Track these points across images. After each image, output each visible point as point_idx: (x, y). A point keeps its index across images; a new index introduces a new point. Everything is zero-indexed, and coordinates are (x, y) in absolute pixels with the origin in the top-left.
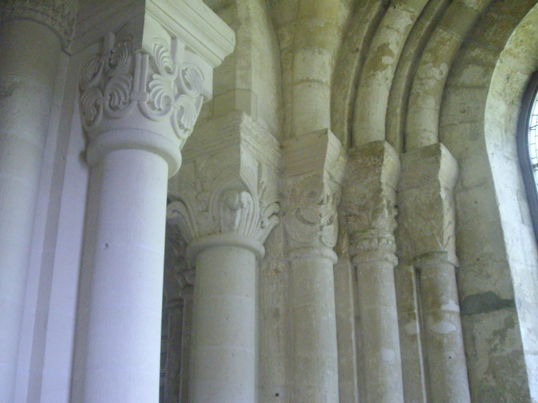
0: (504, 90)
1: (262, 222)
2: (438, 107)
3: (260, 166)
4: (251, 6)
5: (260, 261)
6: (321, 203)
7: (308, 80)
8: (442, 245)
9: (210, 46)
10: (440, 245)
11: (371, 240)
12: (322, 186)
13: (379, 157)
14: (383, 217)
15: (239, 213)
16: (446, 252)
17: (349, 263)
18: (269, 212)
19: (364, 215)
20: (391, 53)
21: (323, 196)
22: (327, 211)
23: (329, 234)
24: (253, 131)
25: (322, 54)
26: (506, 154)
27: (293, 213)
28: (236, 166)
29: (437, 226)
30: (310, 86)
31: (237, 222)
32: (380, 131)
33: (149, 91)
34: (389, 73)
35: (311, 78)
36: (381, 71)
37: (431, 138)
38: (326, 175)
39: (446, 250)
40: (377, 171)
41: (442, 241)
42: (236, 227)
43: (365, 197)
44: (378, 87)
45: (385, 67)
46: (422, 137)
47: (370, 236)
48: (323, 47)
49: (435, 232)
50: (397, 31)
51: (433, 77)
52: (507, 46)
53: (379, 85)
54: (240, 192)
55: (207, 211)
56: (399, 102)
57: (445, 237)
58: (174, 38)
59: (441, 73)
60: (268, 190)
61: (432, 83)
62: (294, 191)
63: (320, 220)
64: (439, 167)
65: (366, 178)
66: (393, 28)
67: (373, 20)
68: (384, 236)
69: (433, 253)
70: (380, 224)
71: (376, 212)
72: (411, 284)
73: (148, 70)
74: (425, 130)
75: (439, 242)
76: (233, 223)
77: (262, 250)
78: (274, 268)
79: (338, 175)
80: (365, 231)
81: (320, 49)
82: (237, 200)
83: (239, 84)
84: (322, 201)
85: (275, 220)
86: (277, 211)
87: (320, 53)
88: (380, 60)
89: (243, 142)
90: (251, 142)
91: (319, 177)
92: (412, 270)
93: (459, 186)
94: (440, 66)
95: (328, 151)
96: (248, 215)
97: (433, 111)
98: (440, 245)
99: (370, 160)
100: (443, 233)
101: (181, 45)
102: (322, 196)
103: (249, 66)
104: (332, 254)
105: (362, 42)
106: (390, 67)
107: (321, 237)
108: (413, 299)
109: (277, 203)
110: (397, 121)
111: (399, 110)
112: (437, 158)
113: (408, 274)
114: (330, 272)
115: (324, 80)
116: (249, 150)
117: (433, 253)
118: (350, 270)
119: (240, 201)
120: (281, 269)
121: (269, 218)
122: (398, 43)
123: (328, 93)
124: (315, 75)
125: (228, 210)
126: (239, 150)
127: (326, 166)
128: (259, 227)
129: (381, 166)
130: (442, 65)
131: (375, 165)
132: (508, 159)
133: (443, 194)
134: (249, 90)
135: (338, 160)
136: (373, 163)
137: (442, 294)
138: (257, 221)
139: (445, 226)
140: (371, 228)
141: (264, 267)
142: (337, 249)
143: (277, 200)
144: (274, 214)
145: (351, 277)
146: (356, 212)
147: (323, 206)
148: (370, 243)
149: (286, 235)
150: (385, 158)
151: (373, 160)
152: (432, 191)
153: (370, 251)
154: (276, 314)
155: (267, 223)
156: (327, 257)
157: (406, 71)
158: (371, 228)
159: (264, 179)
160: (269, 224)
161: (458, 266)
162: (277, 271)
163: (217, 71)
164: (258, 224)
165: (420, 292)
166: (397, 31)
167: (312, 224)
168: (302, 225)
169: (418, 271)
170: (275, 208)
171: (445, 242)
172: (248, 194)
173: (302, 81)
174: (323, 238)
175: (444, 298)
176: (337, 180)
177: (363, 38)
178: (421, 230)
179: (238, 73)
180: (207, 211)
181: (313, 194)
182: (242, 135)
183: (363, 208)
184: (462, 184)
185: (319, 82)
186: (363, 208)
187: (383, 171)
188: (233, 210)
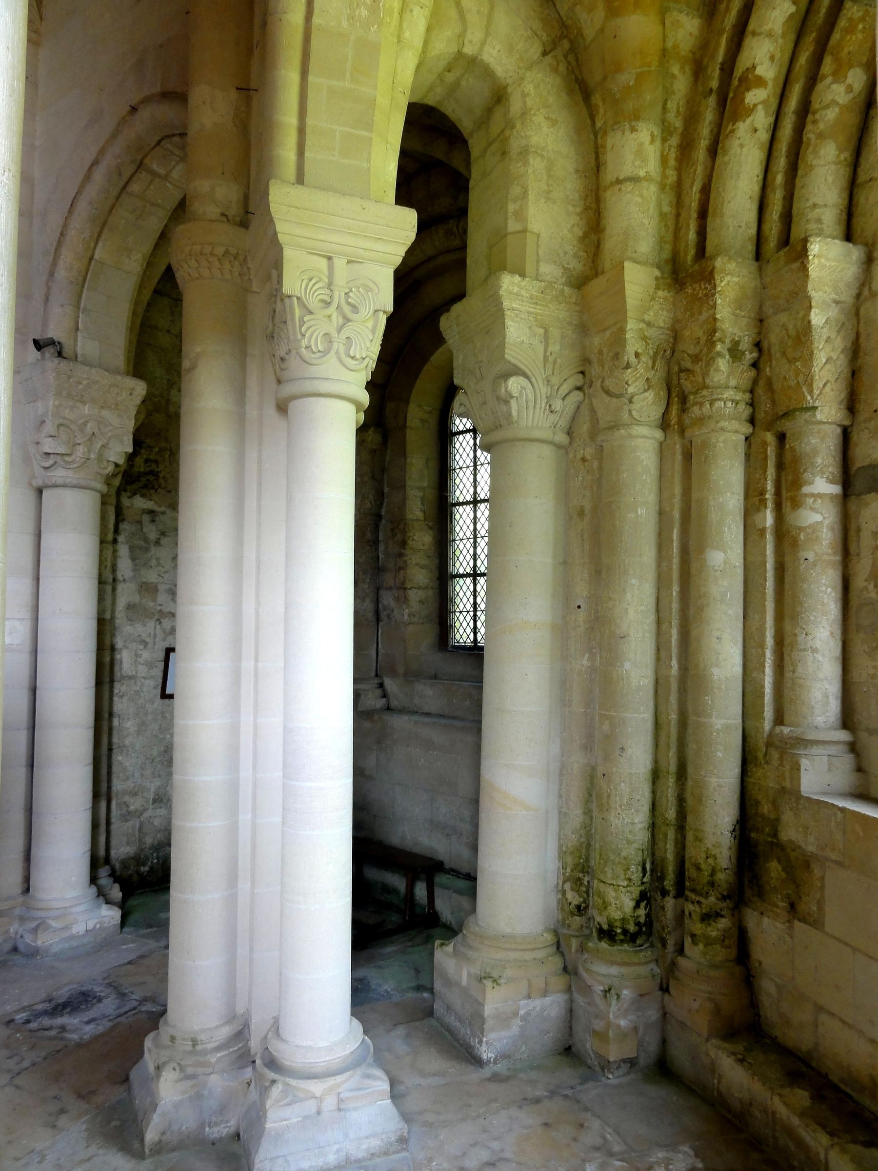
1: (550, 406)
2: (846, 155)
6: (628, 366)
7: (619, 182)
8: (812, 397)
9: (379, 247)
10: (809, 398)
11: (701, 404)
13: (709, 281)
14: (717, 370)
15: (513, 404)
16: (815, 408)
17: (677, 438)
19: (697, 368)
20: (760, 82)
24: (523, 292)
25: (637, 131)
27: (599, 384)
29: (804, 370)
30: (620, 189)
31: (514, 413)
32: (740, 227)
33: (303, 335)
34: (761, 119)
35: (621, 178)
36: (744, 121)
37: (823, 217)
38: (632, 325)
39: (817, 404)
40: (711, 303)
41: (811, 392)
42: (515, 419)
43: (699, 342)
44: (739, 150)
45: (750, 111)
46: (807, 220)
47: (700, 400)
48: (637, 118)
49: (801, 379)
50: (770, 35)
51: (834, 102)
53: (741, 146)
55: (485, 403)
56: (781, 162)
57: (818, 384)
58: (330, 258)
59: (849, 89)
60: (559, 361)
61: (831, 114)
62: (601, 352)
63: (626, 390)
64: (807, 276)
65: (700, 313)
66: (759, 34)
67: (734, 26)
68: (720, 396)
69: (795, 410)
70: (716, 379)
71: (710, 361)
72: (765, 459)
73: (297, 312)
74: (815, 206)
75: (806, 393)
76: (510, 414)
78: (581, 456)
79: (661, 315)
80: (696, 393)
81: (633, 123)
82: (503, 390)
83: (513, 226)
84: (628, 363)
85: (577, 396)
86: (579, 384)
87: (633, 130)
88: (743, 100)
89: (507, 313)
90: (522, 309)
91: (622, 330)
92: (770, 437)
93: (866, 292)
94: (846, 77)
95: (628, 292)
96: (527, 402)
97: (833, 167)
98: (809, 398)
99: (700, 287)
100: (812, 380)
101: (340, 263)
102: (626, 358)
103: (525, 195)
105: (718, 72)
106: (760, 107)
107: (630, 411)
108: (766, 479)
109: (582, 373)
110: (777, 198)
111: (779, 179)
112: (803, 262)
113: (765, 444)
115: (642, 174)
116: (521, 318)
117: (795, 410)
118: (678, 447)
119: (506, 391)
120: (588, 457)
122: (772, 58)
125: (502, 402)
128: (547, 412)
129: (714, 295)
130: (851, 73)
131: (706, 295)
133: (817, 318)
134: (524, 231)
135: (653, 299)
136: (705, 292)
137: (804, 471)
138: (543, 405)
139: (816, 369)
140: (705, 387)
141: (571, 456)
143: (581, 369)
145: (679, 457)
146: (688, 364)
147: (629, 370)
148: (700, 409)
149: (593, 411)
150: (718, 282)
151: (703, 287)
152: (802, 313)
153: (701, 420)
155: (558, 405)
156: (637, 437)
157: (793, 103)
158: (705, 387)
159: (555, 348)
161: (847, 423)
162: (584, 460)
164: (545, 409)
165: (780, 466)
166: (770, 35)
167: (619, 396)
168: (607, 399)
169: (782, 438)
170: (578, 380)
171: (816, 392)
172: (521, 380)
173: (612, 184)
174: (634, 413)
175: (807, 476)
176: (662, 325)
177: (718, 66)
178: (785, 378)
179: (511, 207)
180: (485, 403)
181: (617, 356)
182: (506, 304)
183: (696, 359)
184: (870, 288)
185: (635, 179)
186: (696, 359)
187: (719, 301)
188: (507, 402)
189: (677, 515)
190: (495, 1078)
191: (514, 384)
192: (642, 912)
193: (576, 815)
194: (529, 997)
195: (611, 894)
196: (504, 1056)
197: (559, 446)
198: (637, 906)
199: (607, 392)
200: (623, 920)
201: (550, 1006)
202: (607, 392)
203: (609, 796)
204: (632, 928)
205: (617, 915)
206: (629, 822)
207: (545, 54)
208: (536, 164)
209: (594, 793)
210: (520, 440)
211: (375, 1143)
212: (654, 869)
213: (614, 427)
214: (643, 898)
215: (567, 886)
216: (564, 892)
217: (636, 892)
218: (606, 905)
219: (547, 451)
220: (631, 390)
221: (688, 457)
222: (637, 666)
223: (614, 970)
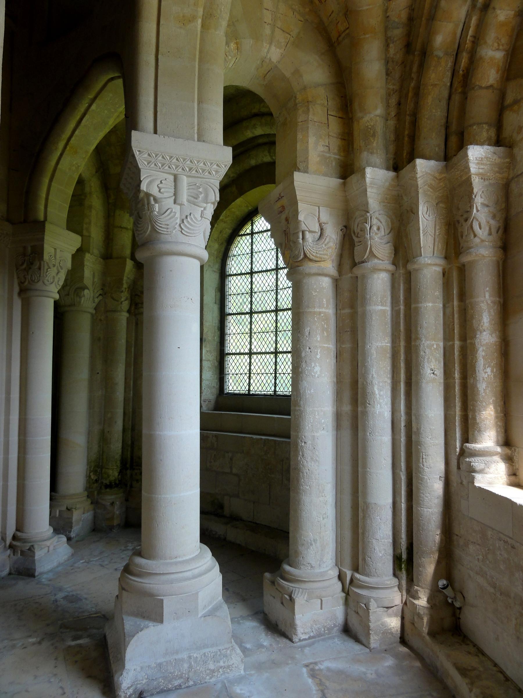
0: (218, 238)
3: (94, 274)
4: (92, 184)
5: (92, 315)
6: (122, 292)
7: (121, 227)
12: (122, 284)
18: (97, 295)
21: (123, 289)
22: (124, 296)
23: (125, 305)
26: (214, 270)
28: (82, 277)
31: (82, 302)
33: (47, 276)
38: (125, 278)
52: (221, 218)
54: (84, 290)
55: (68, 295)
58: (55, 249)
73: (46, 267)
76: (80, 302)
77: (94, 312)
79: (132, 277)
85: (101, 298)
101: (58, 251)
103: (90, 223)
104: (127, 315)
114: (124, 323)
115: (129, 227)
121: (97, 297)
123: (130, 234)
124: (124, 225)
126: (83, 270)
127: (125, 275)
132: (215, 272)
134: (90, 236)
142: (129, 311)
144: (100, 295)
145: (134, 324)
154: (99, 339)
159: (96, 280)
160: (97, 300)
162: (101, 320)
163: (74, 256)
167: (118, 301)
170: (100, 292)
179: (85, 226)
180: (68, 295)
185: (126, 229)
188: (80, 297)
189: (133, 343)
190: (77, 541)
191: (86, 292)
192: (120, 476)
193: (95, 448)
194: (84, 513)
195: (111, 472)
196: (77, 535)
197: (92, 314)
198: (119, 475)
199: (113, 298)
200: (115, 480)
201: (89, 516)
202: (113, 298)
203: (110, 439)
204: (117, 482)
205: (112, 478)
206: (116, 446)
207: (96, 172)
208: (94, 212)
209: (104, 439)
210: (85, 312)
211: (66, 557)
212: (123, 461)
213: (115, 311)
214: (120, 472)
215: (92, 474)
216: (90, 476)
217: (119, 470)
218: (109, 476)
219: (89, 316)
220: (122, 300)
221: (137, 324)
222: (120, 394)
223: (113, 497)
